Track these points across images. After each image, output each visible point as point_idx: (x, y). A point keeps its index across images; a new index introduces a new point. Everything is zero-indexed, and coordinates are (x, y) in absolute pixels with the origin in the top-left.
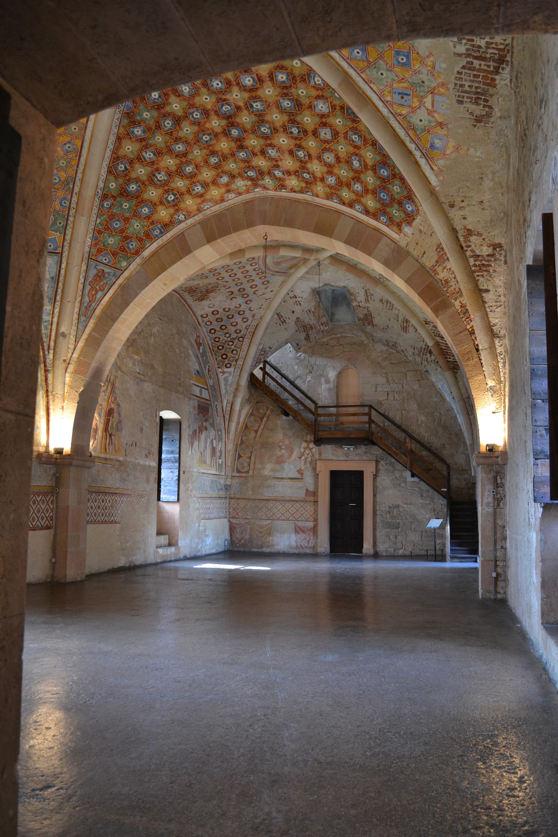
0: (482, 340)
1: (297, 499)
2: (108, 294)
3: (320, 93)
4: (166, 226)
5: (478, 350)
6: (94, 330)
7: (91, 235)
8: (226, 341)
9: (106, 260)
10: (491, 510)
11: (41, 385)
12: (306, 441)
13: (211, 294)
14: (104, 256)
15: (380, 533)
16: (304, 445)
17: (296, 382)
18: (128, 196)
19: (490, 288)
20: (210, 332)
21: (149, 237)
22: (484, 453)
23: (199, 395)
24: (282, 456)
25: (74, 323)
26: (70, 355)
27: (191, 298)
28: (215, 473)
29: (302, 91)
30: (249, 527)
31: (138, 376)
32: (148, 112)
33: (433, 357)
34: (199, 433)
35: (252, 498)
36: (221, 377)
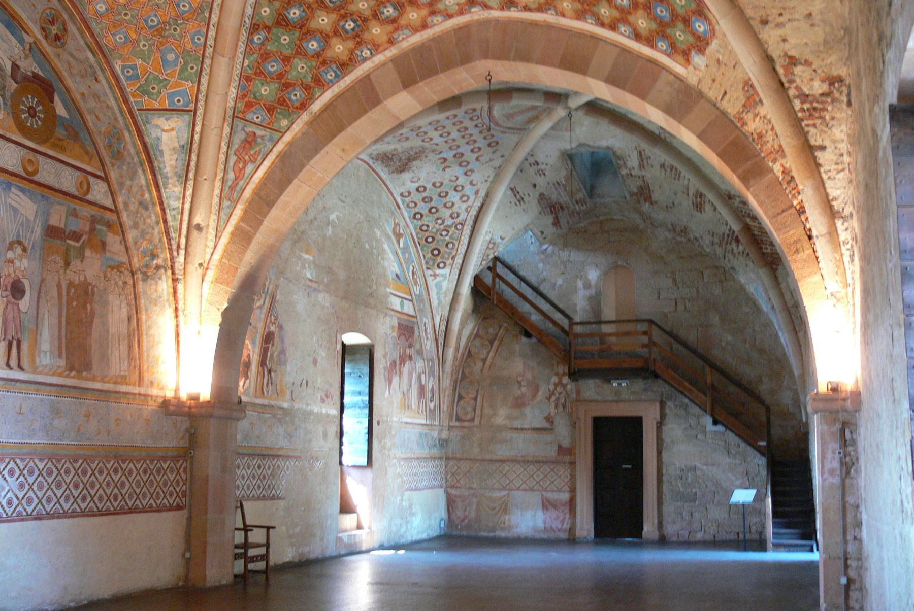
0: (816, 221)
1: (544, 460)
2: (262, 167)
4: (344, 66)
5: (810, 237)
6: (242, 219)
7: (236, 83)
8: (437, 231)
9: (258, 118)
10: (836, 480)
11: (168, 300)
12: (557, 374)
13: (415, 163)
14: (255, 113)
15: (669, 508)
16: (555, 379)
17: (542, 288)
18: (288, 25)
19: (827, 143)
20: (414, 218)
21: (320, 83)
22: (825, 395)
23: (399, 309)
24: (522, 396)
25: (214, 211)
26: (208, 256)
27: (386, 170)
28: (424, 422)
30: (475, 500)
31: (310, 284)
33: (741, 248)
34: (400, 364)
35: (479, 457)
36: (432, 282)
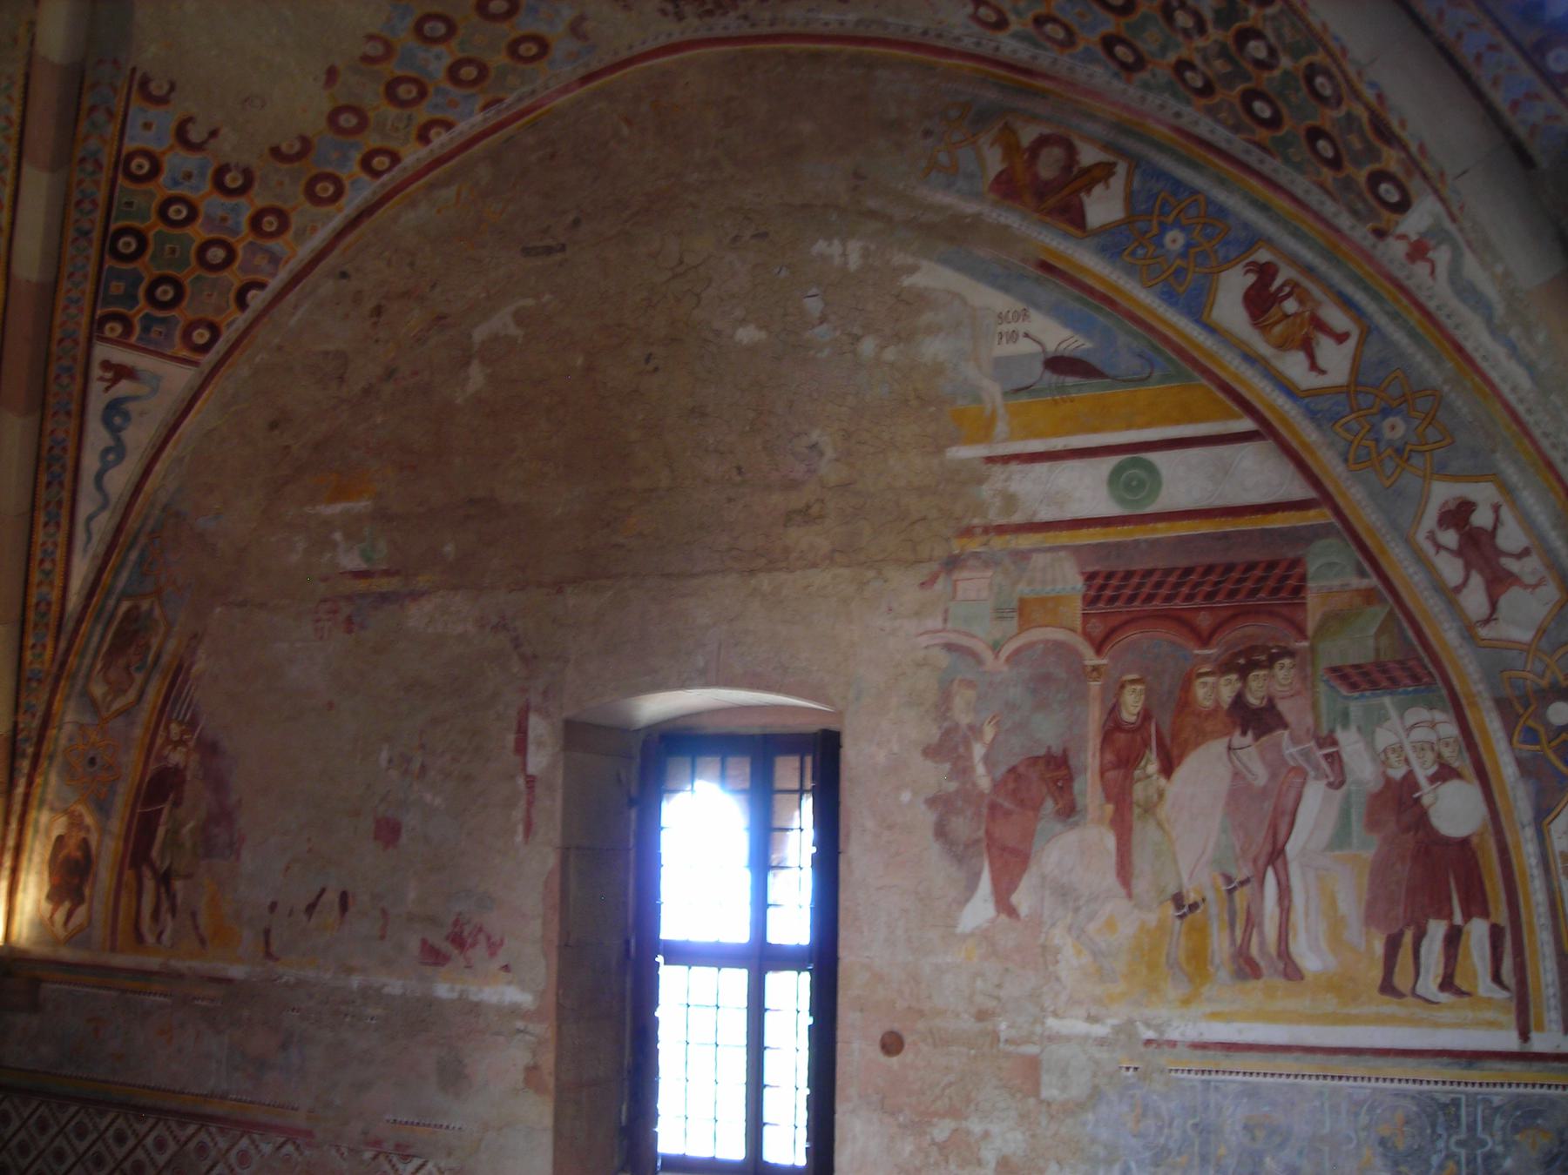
31: (361, 585)
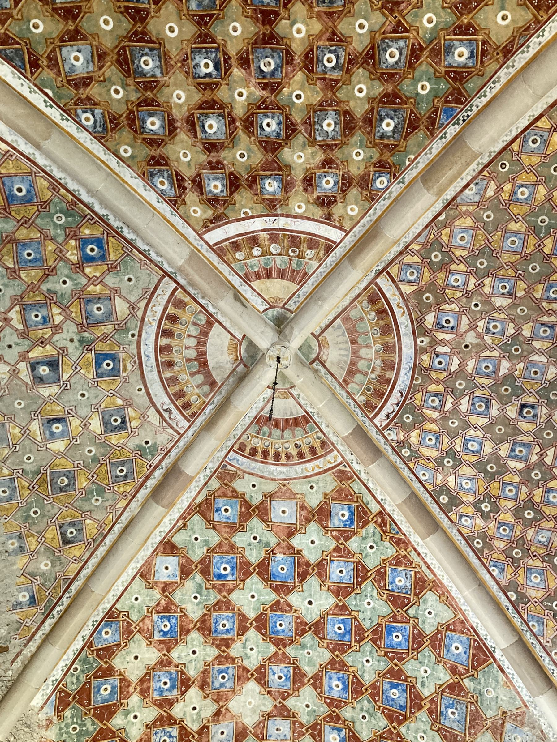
3: (83, 93)
29: (118, 94)
32: (418, 94)
